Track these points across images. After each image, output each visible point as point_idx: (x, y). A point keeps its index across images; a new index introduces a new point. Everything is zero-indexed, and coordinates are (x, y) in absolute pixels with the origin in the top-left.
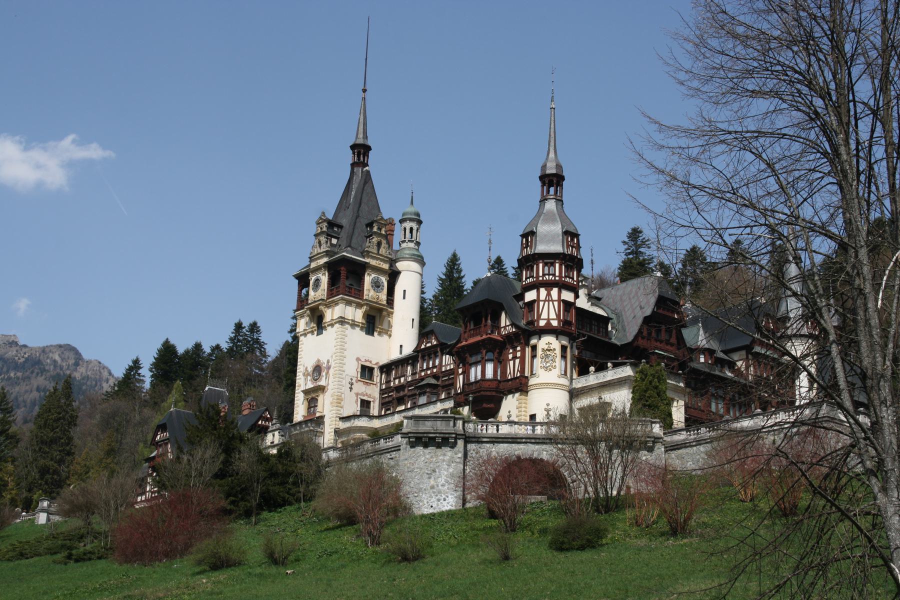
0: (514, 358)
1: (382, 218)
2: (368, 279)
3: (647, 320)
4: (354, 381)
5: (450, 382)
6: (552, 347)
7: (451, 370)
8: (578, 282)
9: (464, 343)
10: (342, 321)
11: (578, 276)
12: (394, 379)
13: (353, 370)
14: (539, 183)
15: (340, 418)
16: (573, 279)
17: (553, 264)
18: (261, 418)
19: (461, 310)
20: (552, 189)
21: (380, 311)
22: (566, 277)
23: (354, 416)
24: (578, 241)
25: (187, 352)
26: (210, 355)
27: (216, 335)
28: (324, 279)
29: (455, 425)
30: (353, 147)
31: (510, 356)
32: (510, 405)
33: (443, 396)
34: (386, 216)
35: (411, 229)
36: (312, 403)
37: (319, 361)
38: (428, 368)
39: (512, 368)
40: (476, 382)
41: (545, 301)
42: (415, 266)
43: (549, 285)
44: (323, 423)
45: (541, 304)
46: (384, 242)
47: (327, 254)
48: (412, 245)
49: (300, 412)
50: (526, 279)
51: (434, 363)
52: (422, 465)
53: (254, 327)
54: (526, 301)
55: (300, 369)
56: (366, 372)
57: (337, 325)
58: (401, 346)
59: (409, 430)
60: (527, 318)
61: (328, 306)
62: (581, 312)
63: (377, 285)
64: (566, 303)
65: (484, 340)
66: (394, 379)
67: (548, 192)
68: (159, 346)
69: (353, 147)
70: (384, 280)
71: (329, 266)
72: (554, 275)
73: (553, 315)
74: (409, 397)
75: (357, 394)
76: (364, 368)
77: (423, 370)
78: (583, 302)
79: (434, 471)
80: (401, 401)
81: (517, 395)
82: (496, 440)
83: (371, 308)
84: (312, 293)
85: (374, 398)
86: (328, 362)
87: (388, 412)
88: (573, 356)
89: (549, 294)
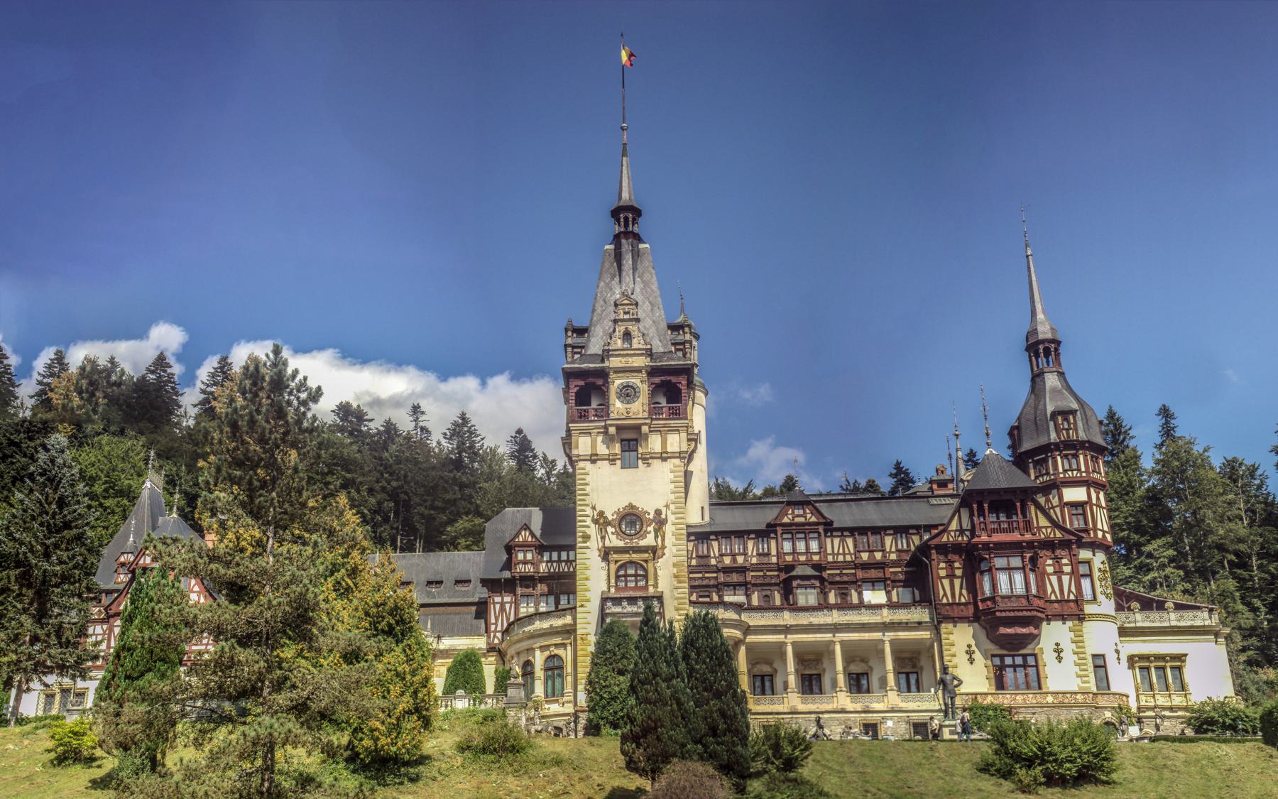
0: (1059, 573)
5: (846, 579)
9: (984, 538)
28: (644, 389)
31: (1050, 570)
33: (832, 598)
49: (594, 579)
50: (1065, 471)
51: (807, 547)
54: (1066, 500)
66: (722, 555)
71: (653, 372)
73: (1106, 529)
74: (755, 585)
81: (1069, 624)
84: (617, 405)
86: (658, 512)
89: (1098, 498)
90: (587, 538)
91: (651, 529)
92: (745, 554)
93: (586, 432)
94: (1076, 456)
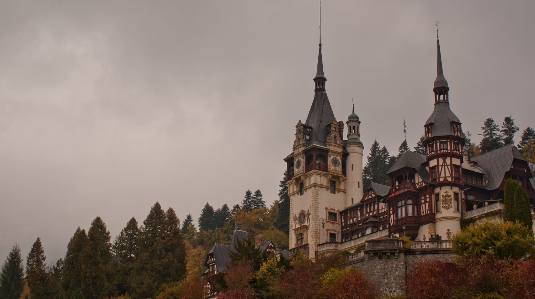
0: (425, 202)
1: (336, 122)
2: (330, 159)
3: (508, 175)
4: (325, 222)
5: (385, 219)
6: (449, 194)
7: (384, 212)
8: (462, 152)
9: (393, 195)
10: (315, 185)
11: (462, 149)
12: (350, 219)
13: (323, 215)
14: (434, 93)
15: (318, 245)
16: (459, 151)
17: (446, 143)
18: (268, 247)
19: (390, 175)
20: (442, 97)
21: (338, 178)
22: (454, 150)
23: (327, 243)
24: (460, 127)
25: (219, 210)
26: (233, 211)
27: (235, 200)
29: (398, 244)
30: (315, 80)
31: (423, 201)
32: (425, 232)
33: (381, 229)
34: (338, 120)
35: (354, 127)
36: (299, 237)
37: (302, 211)
38: (370, 211)
39: (425, 208)
40: (402, 219)
41: (442, 166)
42: (357, 149)
43: (444, 156)
44: (308, 248)
45: (440, 168)
46: (338, 136)
47: (303, 145)
48: (355, 137)
50: (429, 153)
52: (379, 270)
53: (258, 193)
55: (292, 216)
56: (332, 215)
57: (313, 188)
58: (352, 199)
59: (369, 249)
60: (432, 177)
61: (306, 177)
62: (465, 171)
63: (335, 162)
64: (456, 167)
65: (405, 193)
66: (350, 219)
67: (439, 98)
68: (203, 207)
69: (315, 80)
70: (339, 159)
71: (305, 152)
72: (447, 149)
73: (448, 174)
74: (359, 230)
75: (327, 230)
76: (330, 213)
77: (367, 213)
78: (466, 165)
79: (387, 274)
80: (354, 232)
81: (428, 225)
82: (424, 252)
83: (333, 176)
84: (296, 170)
85: (338, 232)
87: (347, 240)
88: (462, 199)
89: (444, 161)
90: (292, 226)
91: (306, 218)
92: (357, 217)
93: (290, 184)
94: (433, 145)
